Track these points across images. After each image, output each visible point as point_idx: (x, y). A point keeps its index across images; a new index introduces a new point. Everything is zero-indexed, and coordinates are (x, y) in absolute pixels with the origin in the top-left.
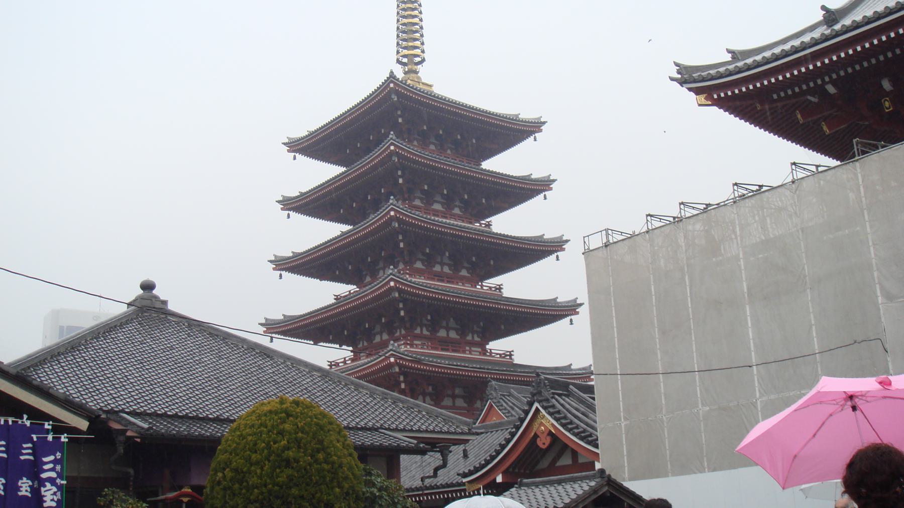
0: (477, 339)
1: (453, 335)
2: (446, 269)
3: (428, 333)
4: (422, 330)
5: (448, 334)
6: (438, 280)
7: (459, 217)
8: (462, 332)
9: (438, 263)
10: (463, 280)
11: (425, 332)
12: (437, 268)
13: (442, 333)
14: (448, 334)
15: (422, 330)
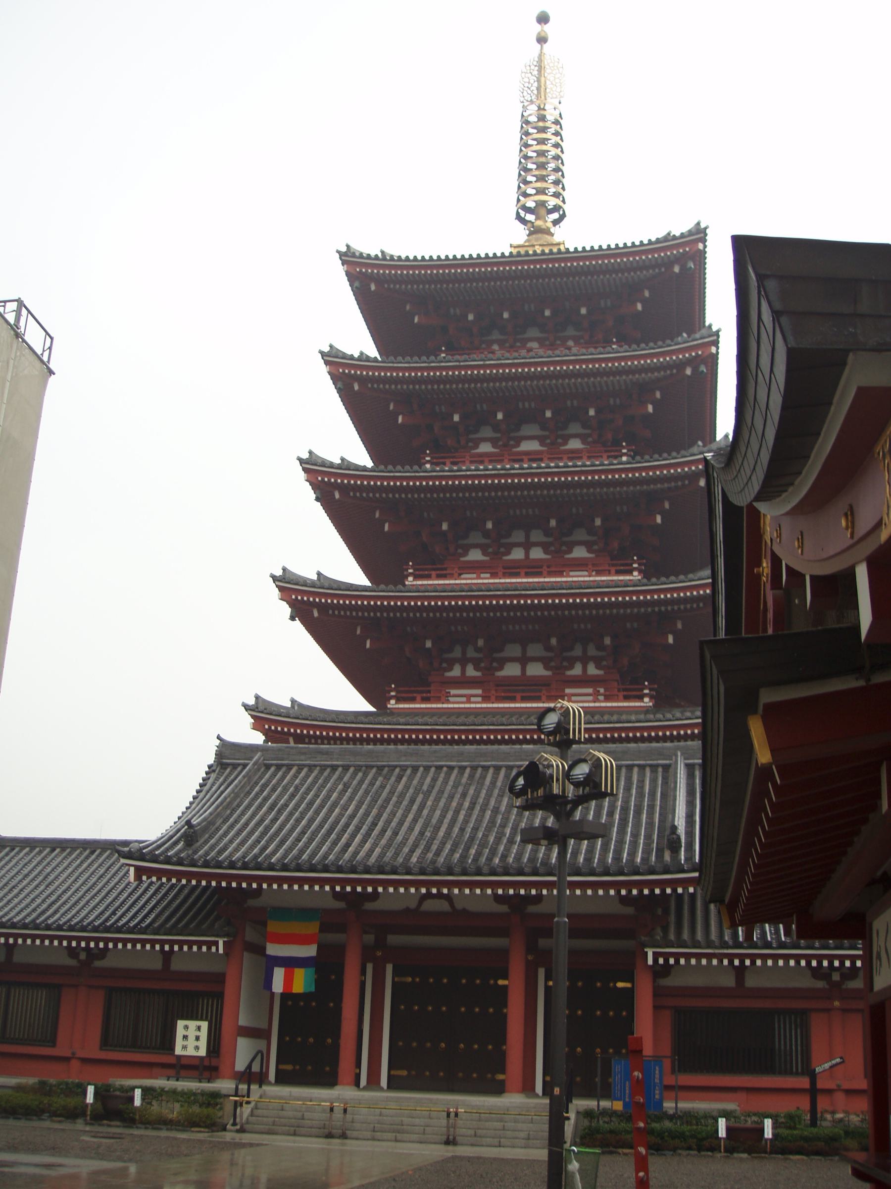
0: (592, 670)
1: (536, 670)
2: (537, 554)
3: (479, 674)
4: (463, 671)
5: (524, 670)
6: (505, 575)
7: (575, 455)
8: (558, 662)
9: (518, 545)
10: (579, 565)
11: (471, 672)
12: (517, 554)
13: (512, 670)
14: (524, 670)
15: (463, 671)
